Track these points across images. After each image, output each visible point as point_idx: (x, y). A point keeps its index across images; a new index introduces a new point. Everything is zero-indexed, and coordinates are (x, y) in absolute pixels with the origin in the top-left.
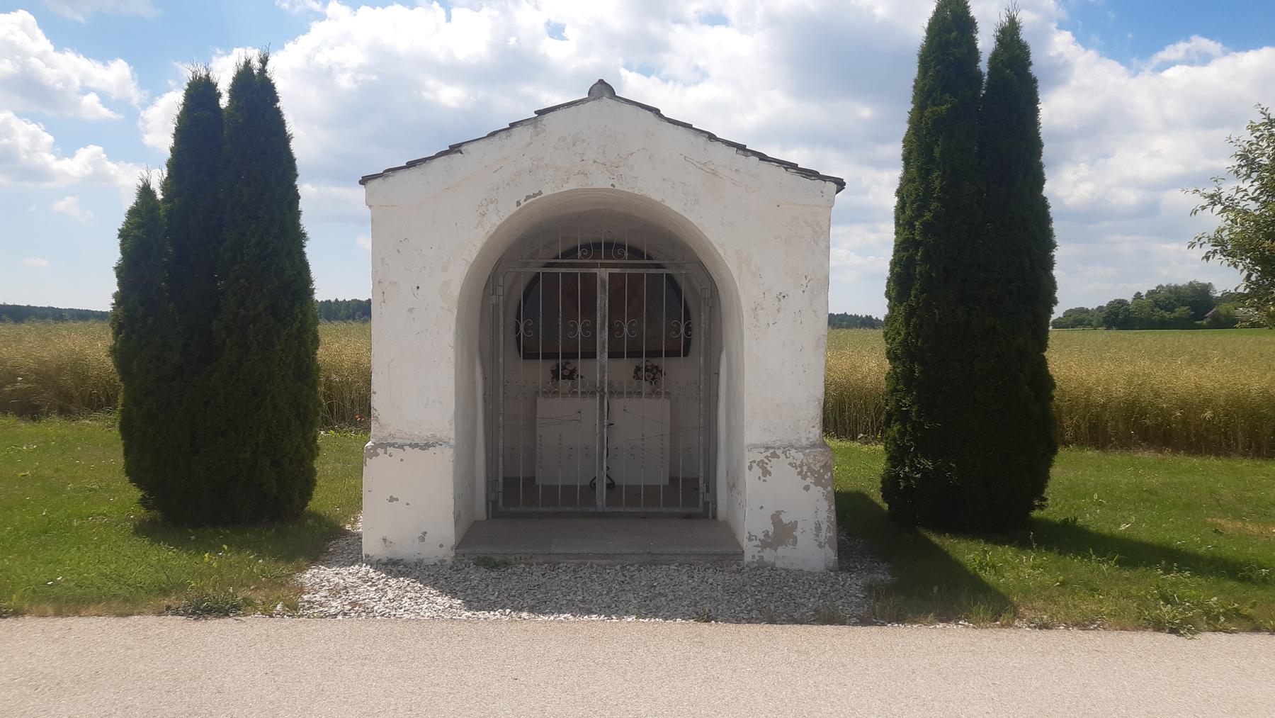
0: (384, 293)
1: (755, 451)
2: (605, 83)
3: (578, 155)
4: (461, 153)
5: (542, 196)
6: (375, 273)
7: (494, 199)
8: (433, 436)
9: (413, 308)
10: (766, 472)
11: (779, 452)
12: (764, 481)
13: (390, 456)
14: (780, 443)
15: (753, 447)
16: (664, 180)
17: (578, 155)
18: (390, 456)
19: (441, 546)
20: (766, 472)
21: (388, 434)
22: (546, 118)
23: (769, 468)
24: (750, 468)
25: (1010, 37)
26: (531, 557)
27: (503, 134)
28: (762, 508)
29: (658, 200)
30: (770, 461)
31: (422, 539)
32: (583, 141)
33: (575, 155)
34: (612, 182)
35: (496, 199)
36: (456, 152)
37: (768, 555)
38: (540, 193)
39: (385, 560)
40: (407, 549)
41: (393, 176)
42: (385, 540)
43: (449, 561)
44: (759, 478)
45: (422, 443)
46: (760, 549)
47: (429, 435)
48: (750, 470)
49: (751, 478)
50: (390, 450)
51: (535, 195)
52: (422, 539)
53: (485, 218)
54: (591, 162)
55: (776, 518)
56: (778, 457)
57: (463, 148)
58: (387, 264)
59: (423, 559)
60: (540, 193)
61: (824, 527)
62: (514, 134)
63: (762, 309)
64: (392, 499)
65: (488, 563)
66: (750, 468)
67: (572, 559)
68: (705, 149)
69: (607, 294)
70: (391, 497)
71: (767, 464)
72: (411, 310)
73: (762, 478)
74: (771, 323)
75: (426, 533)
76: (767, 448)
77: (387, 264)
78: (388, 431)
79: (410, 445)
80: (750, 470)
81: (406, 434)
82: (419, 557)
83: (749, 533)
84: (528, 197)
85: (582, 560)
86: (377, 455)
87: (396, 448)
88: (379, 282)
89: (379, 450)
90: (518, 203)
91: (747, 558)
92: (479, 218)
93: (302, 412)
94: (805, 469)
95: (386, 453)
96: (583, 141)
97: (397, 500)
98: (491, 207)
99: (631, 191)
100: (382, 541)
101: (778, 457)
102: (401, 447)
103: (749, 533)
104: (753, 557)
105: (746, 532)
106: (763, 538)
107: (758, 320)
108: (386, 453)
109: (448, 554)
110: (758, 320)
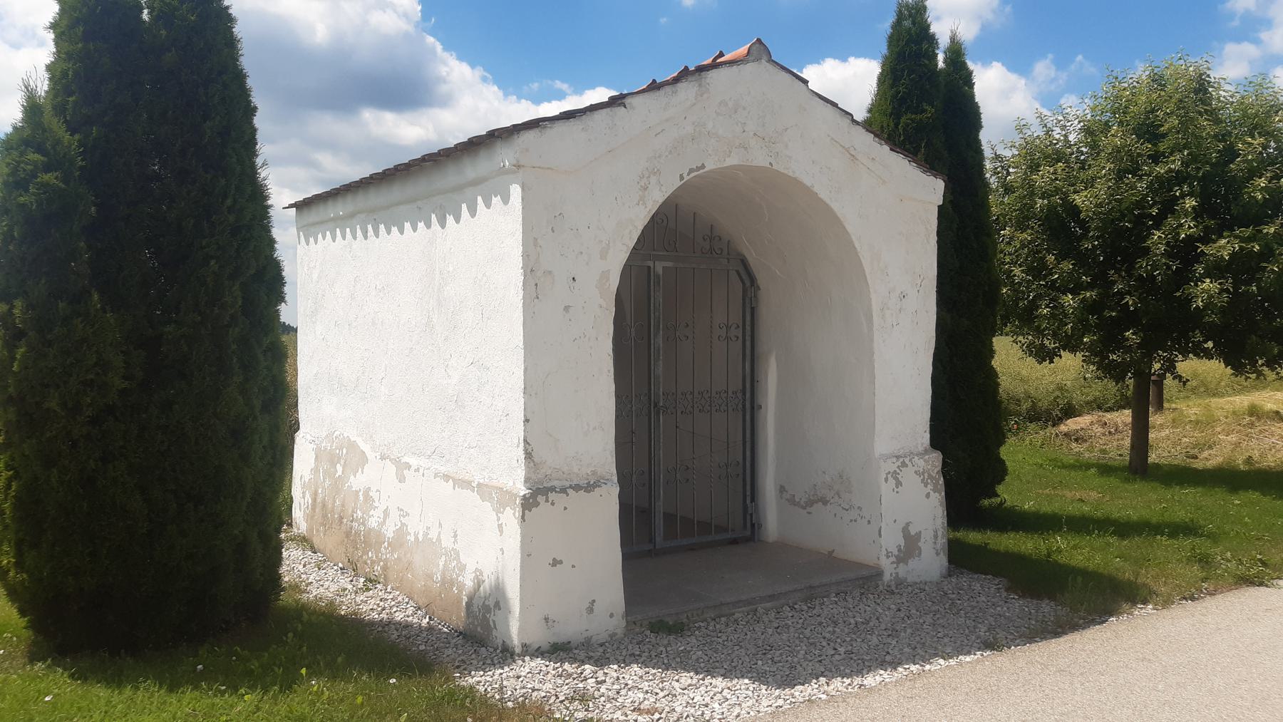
0: (536, 285)
1: (889, 461)
2: (764, 44)
3: (739, 124)
4: (625, 107)
5: (706, 170)
6: (526, 256)
7: (656, 170)
8: (594, 473)
9: (569, 306)
10: (899, 484)
11: (907, 460)
12: (897, 492)
13: (553, 504)
14: (902, 451)
15: (886, 458)
16: (813, 162)
17: (739, 124)
18: (553, 504)
19: (612, 616)
20: (899, 484)
21: (543, 476)
22: (709, 76)
23: (900, 479)
24: (886, 480)
25: (956, 53)
26: (703, 612)
27: (668, 89)
28: (895, 521)
29: (809, 184)
30: (901, 471)
31: (590, 610)
32: (744, 109)
33: (737, 124)
34: (770, 160)
35: (658, 170)
36: (619, 105)
37: (902, 570)
38: (703, 166)
39: (545, 647)
40: (573, 627)
41: (551, 127)
42: (546, 619)
43: (620, 632)
44: (893, 490)
45: (583, 483)
46: (895, 565)
47: (588, 472)
48: (886, 483)
49: (886, 489)
50: (552, 496)
51: (698, 169)
52: (590, 610)
53: (646, 193)
54: (752, 133)
55: (905, 530)
56: (907, 466)
57: (628, 101)
58: (540, 246)
59: (592, 637)
60: (703, 166)
61: (940, 533)
62: (679, 90)
63: (888, 309)
64: (555, 563)
65: (659, 627)
66: (886, 480)
67: (741, 607)
68: (848, 132)
69: (661, 291)
70: (554, 559)
71: (899, 474)
72: (567, 308)
73: (896, 490)
74: (895, 324)
75: (594, 601)
76: (898, 457)
77: (540, 246)
78: (544, 471)
79: (571, 487)
80: (886, 483)
81: (563, 473)
82: (585, 635)
83: (886, 550)
84: (691, 171)
85: (751, 607)
86: (537, 504)
87: (559, 492)
88: (532, 271)
89: (541, 499)
90: (682, 177)
91: (887, 577)
92: (641, 193)
93: (91, 461)
94: (926, 475)
95: (547, 501)
96: (744, 109)
97: (561, 562)
98: (653, 179)
99: (786, 172)
100: (544, 621)
101: (907, 466)
102: (563, 490)
103: (886, 550)
104: (891, 575)
105: (884, 549)
106: (897, 553)
107: (884, 321)
108: (547, 501)
109: (617, 624)
110: (884, 321)
